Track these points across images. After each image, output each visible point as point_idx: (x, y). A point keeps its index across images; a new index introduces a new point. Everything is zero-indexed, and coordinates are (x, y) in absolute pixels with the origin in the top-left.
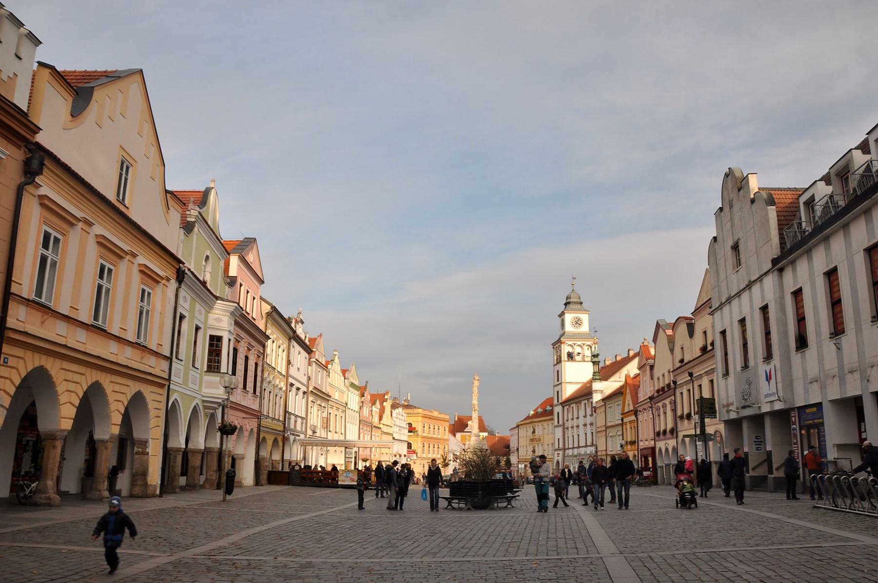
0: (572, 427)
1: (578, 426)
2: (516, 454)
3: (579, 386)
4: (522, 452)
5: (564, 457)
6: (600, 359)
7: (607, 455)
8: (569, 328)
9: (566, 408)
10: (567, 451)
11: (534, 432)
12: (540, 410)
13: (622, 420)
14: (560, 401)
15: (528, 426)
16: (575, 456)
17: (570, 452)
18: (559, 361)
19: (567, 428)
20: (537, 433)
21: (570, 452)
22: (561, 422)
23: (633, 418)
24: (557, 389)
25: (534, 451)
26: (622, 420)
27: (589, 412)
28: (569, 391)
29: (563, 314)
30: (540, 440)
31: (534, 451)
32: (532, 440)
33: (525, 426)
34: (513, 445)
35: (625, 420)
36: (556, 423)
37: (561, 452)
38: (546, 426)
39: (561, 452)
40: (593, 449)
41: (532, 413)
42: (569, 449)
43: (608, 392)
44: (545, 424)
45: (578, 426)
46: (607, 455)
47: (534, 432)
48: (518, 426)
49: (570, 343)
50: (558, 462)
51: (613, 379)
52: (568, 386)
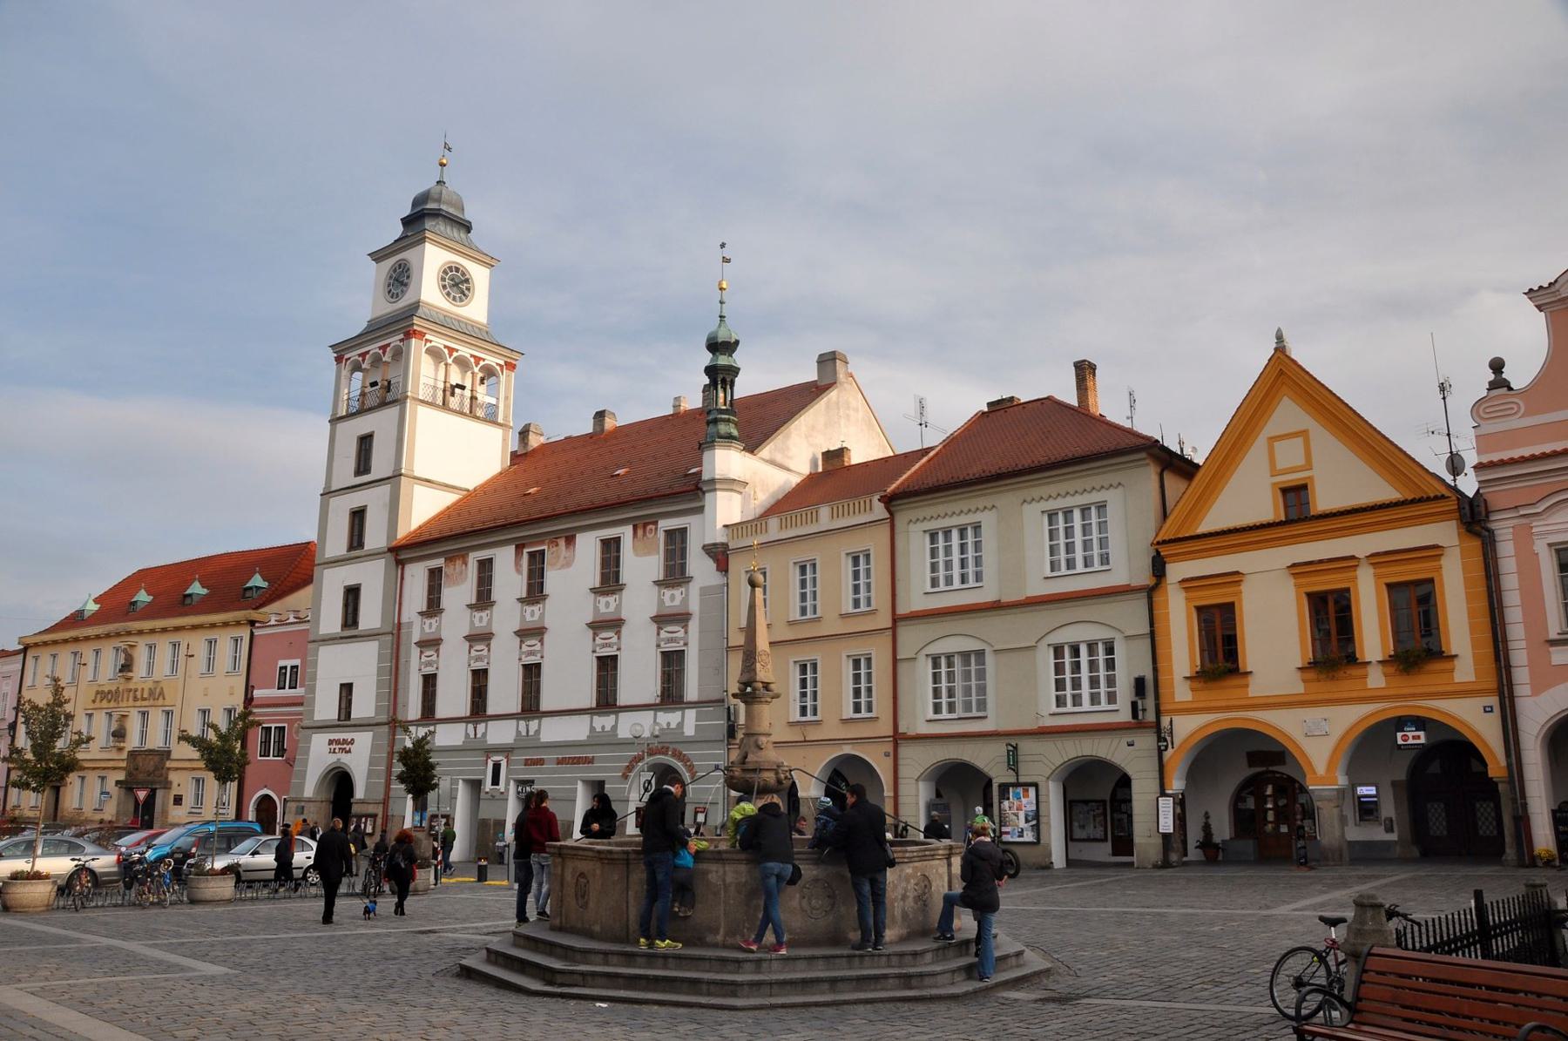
0: (479, 638)
3: (450, 498)
6: (739, 358)
7: (898, 738)
8: (430, 291)
13: (1159, 567)
15: (87, 651)
16: (507, 750)
18: (387, 395)
20: (140, 669)
23: (1444, 533)
26: (1159, 567)
27: (641, 566)
28: (423, 508)
31: (120, 734)
35: (1177, 571)
40: (689, 722)
41: (93, 607)
43: (762, 498)
46: (898, 738)
47: (127, 667)
48: (25, 650)
49: (438, 342)
51: (766, 451)
52: (419, 491)
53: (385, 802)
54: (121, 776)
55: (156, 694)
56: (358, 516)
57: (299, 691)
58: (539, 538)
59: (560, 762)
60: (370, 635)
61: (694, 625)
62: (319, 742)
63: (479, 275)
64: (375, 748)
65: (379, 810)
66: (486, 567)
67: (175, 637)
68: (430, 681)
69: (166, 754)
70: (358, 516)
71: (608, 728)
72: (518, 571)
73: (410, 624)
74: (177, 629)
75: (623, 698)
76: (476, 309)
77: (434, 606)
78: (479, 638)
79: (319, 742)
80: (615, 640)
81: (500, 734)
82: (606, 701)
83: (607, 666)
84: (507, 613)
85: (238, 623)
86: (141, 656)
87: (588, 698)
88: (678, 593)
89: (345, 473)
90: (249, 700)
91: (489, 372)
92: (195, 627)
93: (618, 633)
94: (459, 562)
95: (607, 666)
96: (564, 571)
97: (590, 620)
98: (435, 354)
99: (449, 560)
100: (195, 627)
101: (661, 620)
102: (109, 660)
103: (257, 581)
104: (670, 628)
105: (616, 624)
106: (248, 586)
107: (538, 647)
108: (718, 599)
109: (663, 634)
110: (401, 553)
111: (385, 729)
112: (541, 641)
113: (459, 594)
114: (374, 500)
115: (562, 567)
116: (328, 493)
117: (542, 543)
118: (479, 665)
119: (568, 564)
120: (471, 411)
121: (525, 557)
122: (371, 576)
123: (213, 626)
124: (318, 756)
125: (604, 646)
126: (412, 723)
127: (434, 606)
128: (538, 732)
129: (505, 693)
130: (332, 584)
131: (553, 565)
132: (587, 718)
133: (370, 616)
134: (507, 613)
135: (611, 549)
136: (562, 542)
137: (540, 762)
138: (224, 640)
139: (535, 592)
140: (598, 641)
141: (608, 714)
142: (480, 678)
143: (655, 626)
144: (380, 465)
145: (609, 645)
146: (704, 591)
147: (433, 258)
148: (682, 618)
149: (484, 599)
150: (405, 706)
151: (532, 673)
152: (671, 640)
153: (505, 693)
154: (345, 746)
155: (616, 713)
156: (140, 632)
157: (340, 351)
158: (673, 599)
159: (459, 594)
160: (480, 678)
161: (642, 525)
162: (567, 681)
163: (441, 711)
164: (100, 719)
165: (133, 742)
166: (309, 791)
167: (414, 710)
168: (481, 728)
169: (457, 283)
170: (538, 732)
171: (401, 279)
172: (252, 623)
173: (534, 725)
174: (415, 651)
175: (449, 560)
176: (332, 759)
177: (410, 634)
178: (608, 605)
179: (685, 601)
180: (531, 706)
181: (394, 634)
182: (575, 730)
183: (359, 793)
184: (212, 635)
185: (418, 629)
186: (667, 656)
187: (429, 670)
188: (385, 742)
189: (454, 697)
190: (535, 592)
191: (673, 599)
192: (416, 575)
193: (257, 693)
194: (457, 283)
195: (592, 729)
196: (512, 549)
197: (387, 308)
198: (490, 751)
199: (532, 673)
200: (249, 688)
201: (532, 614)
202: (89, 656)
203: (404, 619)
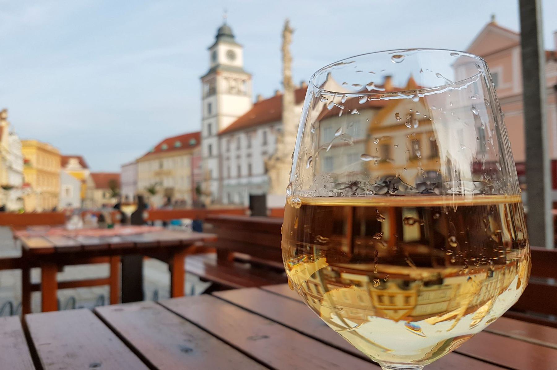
0: (238, 157)
1: (249, 155)
5: (221, 187)
8: (223, 59)
10: (226, 182)
14: (214, 131)
18: (213, 91)
19: (228, 159)
21: (233, 182)
24: (207, 122)
28: (226, 122)
29: (216, 44)
42: (229, 177)
63: (238, 51)
76: (238, 62)
78: (238, 157)
81: (244, 181)
84: (244, 152)
91: (244, 81)
98: (226, 78)
106: (187, 143)
110: (221, 135)
113: (233, 146)
114: (212, 121)
120: (239, 93)
122: (214, 141)
127: (228, 150)
129: (244, 171)
130: (205, 143)
133: (215, 152)
134: (244, 152)
135: (265, 134)
139: (249, 146)
142: (239, 168)
147: (223, 49)
149: (238, 148)
153: (244, 171)
157: (203, 78)
159: (233, 146)
160: (239, 168)
161: (272, 127)
169: (231, 55)
171: (214, 56)
180: (250, 175)
185: (225, 155)
189: (234, 173)
190: (249, 146)
192: (224, 140)
194: (231, 55)
197: (213, 65)
199: (250, 167)
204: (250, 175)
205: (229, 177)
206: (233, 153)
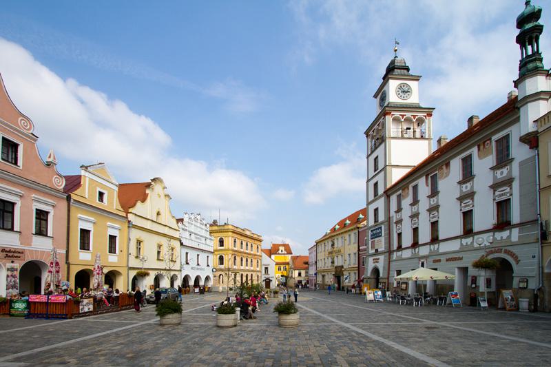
0: (415, 216)
1: (434, 209)
2: (314, 267)
4: (320, 265)
9: (394, 199)
10: (395, 256)
11: (333, 245)
12: (337, 227)
14: (381, 191)
15: (326, 242)
16: (426, 257)
17: (407, 254)
19: (399, 222)
20: (336, 244)
22: (381, 218)
25: (333, 262)
28: (396, 175)
30: (339, 251)
31: (333, 262)
32: (330, 253)
33: (323, 243)
34: (312, 260)
36: (371, 222)
37: (382, 258)
38: (347, 237)
39: (382, 258)
44: (346, 236)
45: (434, 209)
47: (333, 245)
50: (376, 271)
53: (388, 278)
54: (334, 273)
55: (339, 251)
56: (376, 185)
57: (365, 247)
58: (434, 169)
59: (447, 260)
60: (382, 223)
61: (516, 185)
62: (371, 259)
64: (385, 260)
65: (386, 281)
66: (415, 188)
67: (342, 235)
68: (400, 235)
69: (342, 267)
70: (376, 185)
71: (469, 243)
72: (427, 185)
73: (393, 217)
74: (342, 233)
75: (476, 228)
77: (399, 210)
78: (415, 216)
79: (371, 259)
80: (471, 202)
82: (468, 232)
83: (468, 216)
85: (355, 229)
86: (335, 241)
87: (459, 230)
88: (505, 171)
89: (372, 173)
90: (359, 250)
92: (345, 232)
93: (473, 199)
94: (406, 190)
95: (468, 216)
96: (447, 178)
97: (458, 196)
99: (403, 190)
100: (345, 232)
101: (495, 187)
102: (330, 244)
103: (361, 216)
104: (500, 190)
105: (471, 195)
107: (437, 214)
108: (530, 167)
109: (497, 193)
110: (388, 193)
111: (388, 254)
112: (438, 211)
114: (380, 178)
115: (445, 177)
116: (368, 181)
117: (436, 170)
118: (415, 226)
119: (447, 175)
121: (430, 179)
122: (380, 204)
123: (349, 231)
124: (370, 265)
125: (465, 207)
126: (395, 251)
127: (399, 210)
128: (438, 248)
129: (425, 236)
131: (441, 178)
132: (458, 241)
136: (444, 167)
137: (439, 261)
138: (352, 234)
139: (434, 193)
140: (463, 205)
141: (469, 237)
142: (416, 230)
143: (492, 190)
144: (381, 166)
145: (468, 206)
146: (521, 164)
148: (508, 182)
149: (415, 202)
150: (393, 245)
151: (434, 225)
152: (502, 195)
154: (376, 261)
155: (473, 236)
156: (335, 236)
158: (502, 174)
160: (416, 230)
162: (451, 224)
163: (403, 246)
164: (330, 258)
165: (336, 264)
166: (369, 275)
167: (395, 246)
168: (417, 250)
170: (438, 248)
172: (358, 228)
173: (436, 246)
174: (395, 225)
175: (403, 190)
176: (373, 265)
177: (393, 220)
178: (466, 188)
179: (510, 172)
181: (389, 219)
182: (454, 246)
183: (381, 275)
184: (349, 233)
185: (395, 217)
186: (499, 204)
187: (399, 231)
188: (387, 258)
189: (407, 240)
190: (434, 193)
191: (502, 174)
193: (361, 248)
195: (462, 244)
196: (424, 177)
198: (420, 258)
199: (434, 225)
200: (359, 247)
201: (433, 201)
202: (326, 244)
203: (391, 215)
204: (435, 240)
205: (400, 248)
206: (407, 211)
